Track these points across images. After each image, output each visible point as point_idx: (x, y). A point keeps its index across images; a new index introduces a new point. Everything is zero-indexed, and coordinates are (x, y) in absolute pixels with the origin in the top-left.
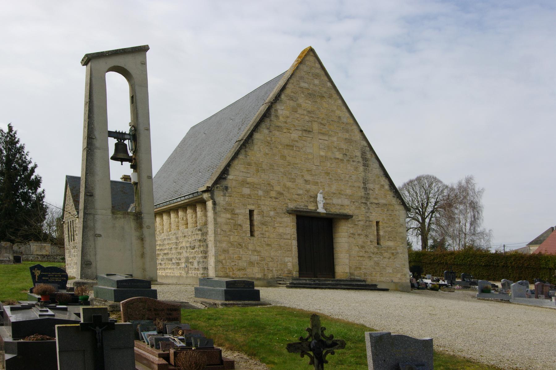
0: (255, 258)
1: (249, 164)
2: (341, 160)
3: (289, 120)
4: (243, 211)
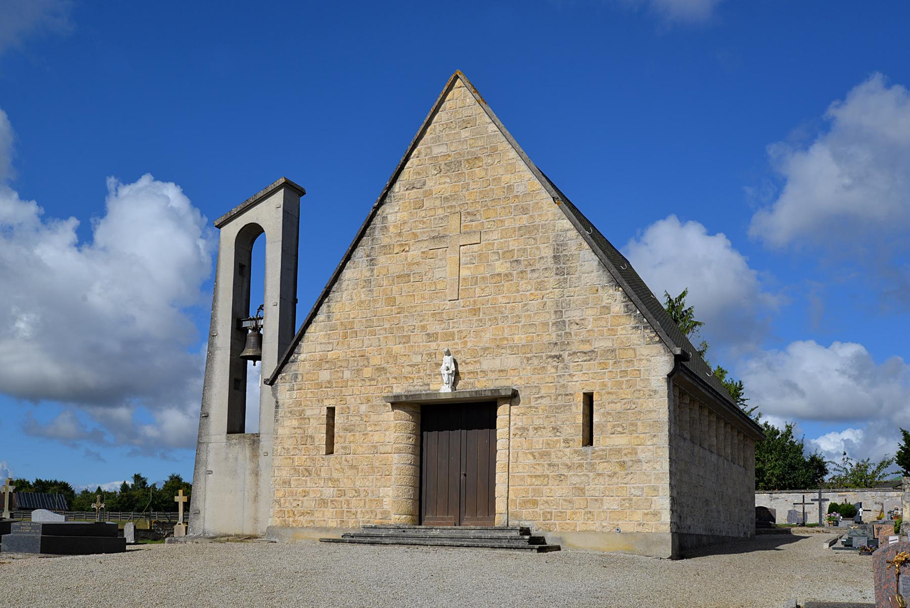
0: (329, 492)
1: (333, 328)
2: (506, 275)
3: (406, 228)
4: (317, 411)
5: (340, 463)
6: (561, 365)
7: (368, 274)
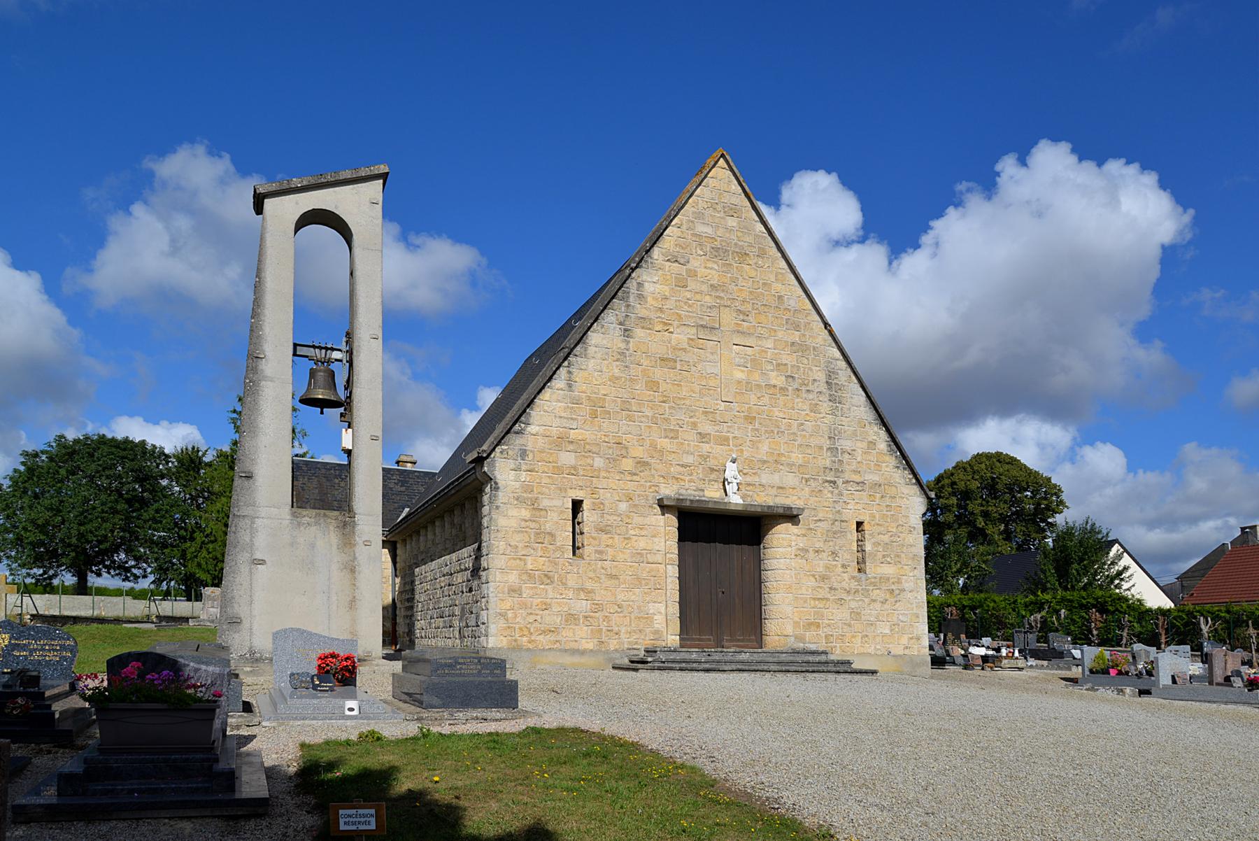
0: (582, 606)
1: (578, 402)
2: (781, 388)
3: (670, 304)
4: (557, 503)
5: (595, 571)
6: (836, 491)
7: (623, 346)
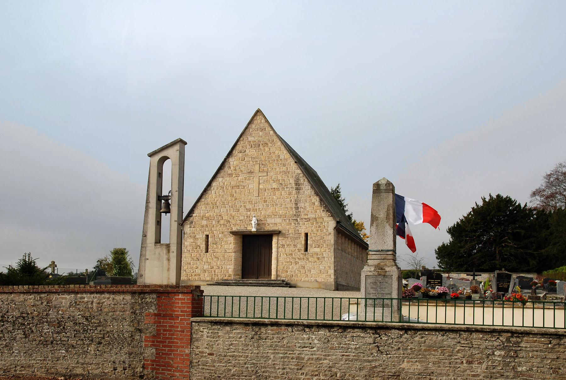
0: (206, 267)
